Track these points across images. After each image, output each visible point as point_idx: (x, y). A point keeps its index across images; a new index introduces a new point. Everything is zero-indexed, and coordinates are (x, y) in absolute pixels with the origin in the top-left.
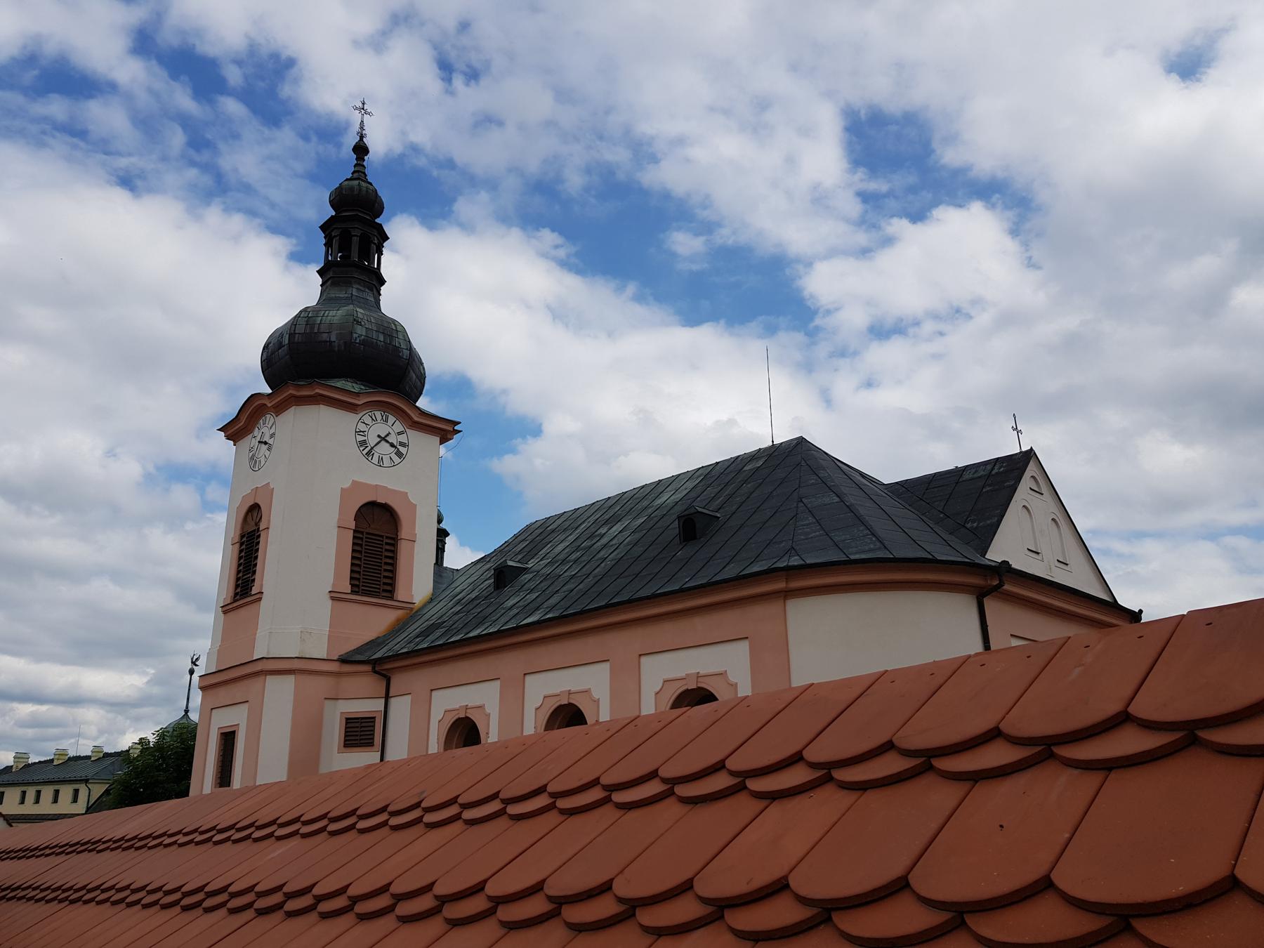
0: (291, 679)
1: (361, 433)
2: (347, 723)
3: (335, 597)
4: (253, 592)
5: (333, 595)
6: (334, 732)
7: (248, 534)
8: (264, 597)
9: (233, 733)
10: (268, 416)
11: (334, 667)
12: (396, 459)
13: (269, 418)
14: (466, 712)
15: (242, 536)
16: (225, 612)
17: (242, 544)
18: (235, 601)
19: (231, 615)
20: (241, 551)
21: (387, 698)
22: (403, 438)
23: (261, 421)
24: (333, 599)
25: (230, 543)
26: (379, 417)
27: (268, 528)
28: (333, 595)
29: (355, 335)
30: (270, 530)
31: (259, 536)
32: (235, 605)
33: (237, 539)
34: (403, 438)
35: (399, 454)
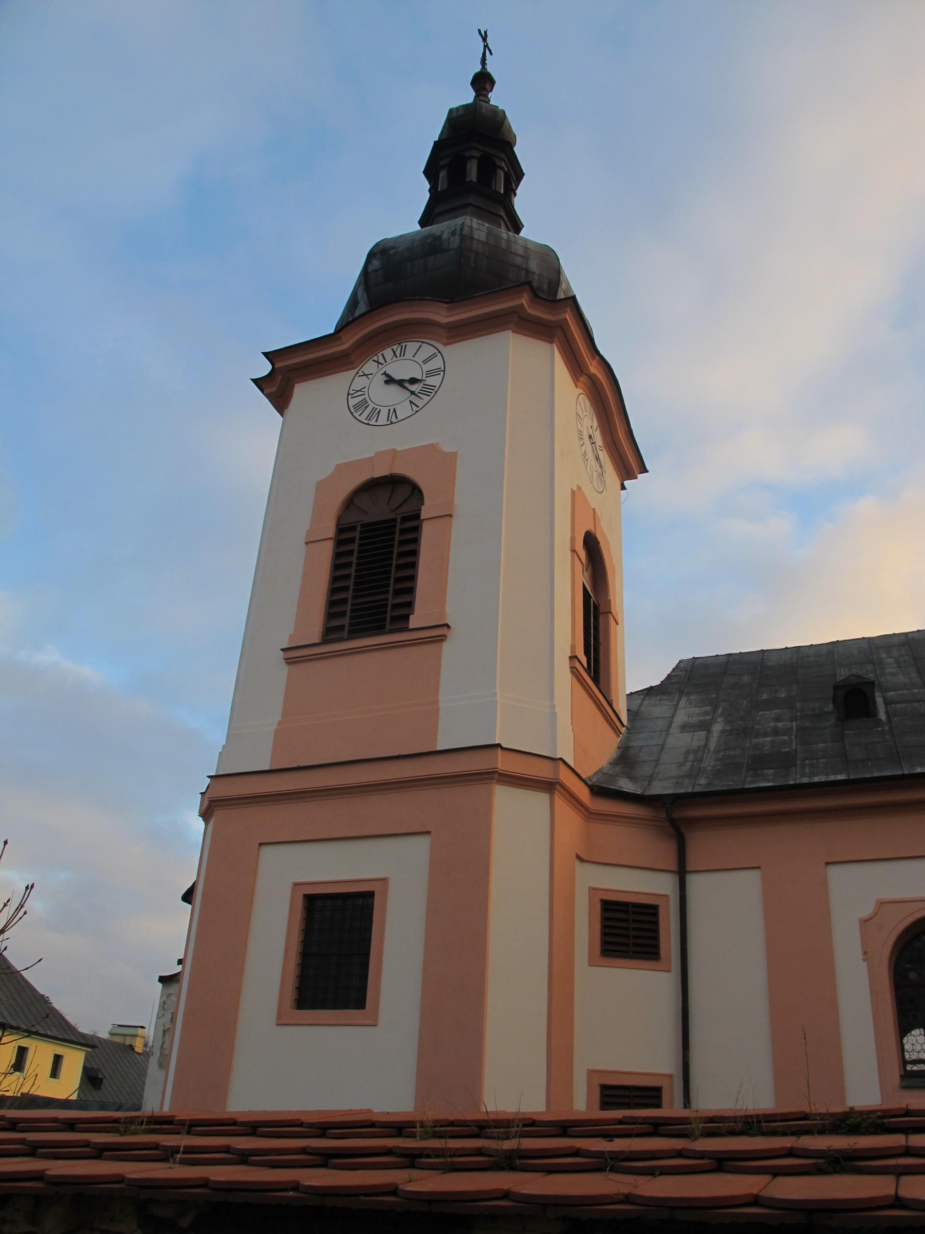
0: (539, 801)
4: (414, 622)
7: (363, 526)
9: (370, 895)
10: (412, 347)
21: (682, 873)
23: (388, 353)
24: (573, 670)
25: (302, 541)
30: (454, 520)
31: (417, 529)
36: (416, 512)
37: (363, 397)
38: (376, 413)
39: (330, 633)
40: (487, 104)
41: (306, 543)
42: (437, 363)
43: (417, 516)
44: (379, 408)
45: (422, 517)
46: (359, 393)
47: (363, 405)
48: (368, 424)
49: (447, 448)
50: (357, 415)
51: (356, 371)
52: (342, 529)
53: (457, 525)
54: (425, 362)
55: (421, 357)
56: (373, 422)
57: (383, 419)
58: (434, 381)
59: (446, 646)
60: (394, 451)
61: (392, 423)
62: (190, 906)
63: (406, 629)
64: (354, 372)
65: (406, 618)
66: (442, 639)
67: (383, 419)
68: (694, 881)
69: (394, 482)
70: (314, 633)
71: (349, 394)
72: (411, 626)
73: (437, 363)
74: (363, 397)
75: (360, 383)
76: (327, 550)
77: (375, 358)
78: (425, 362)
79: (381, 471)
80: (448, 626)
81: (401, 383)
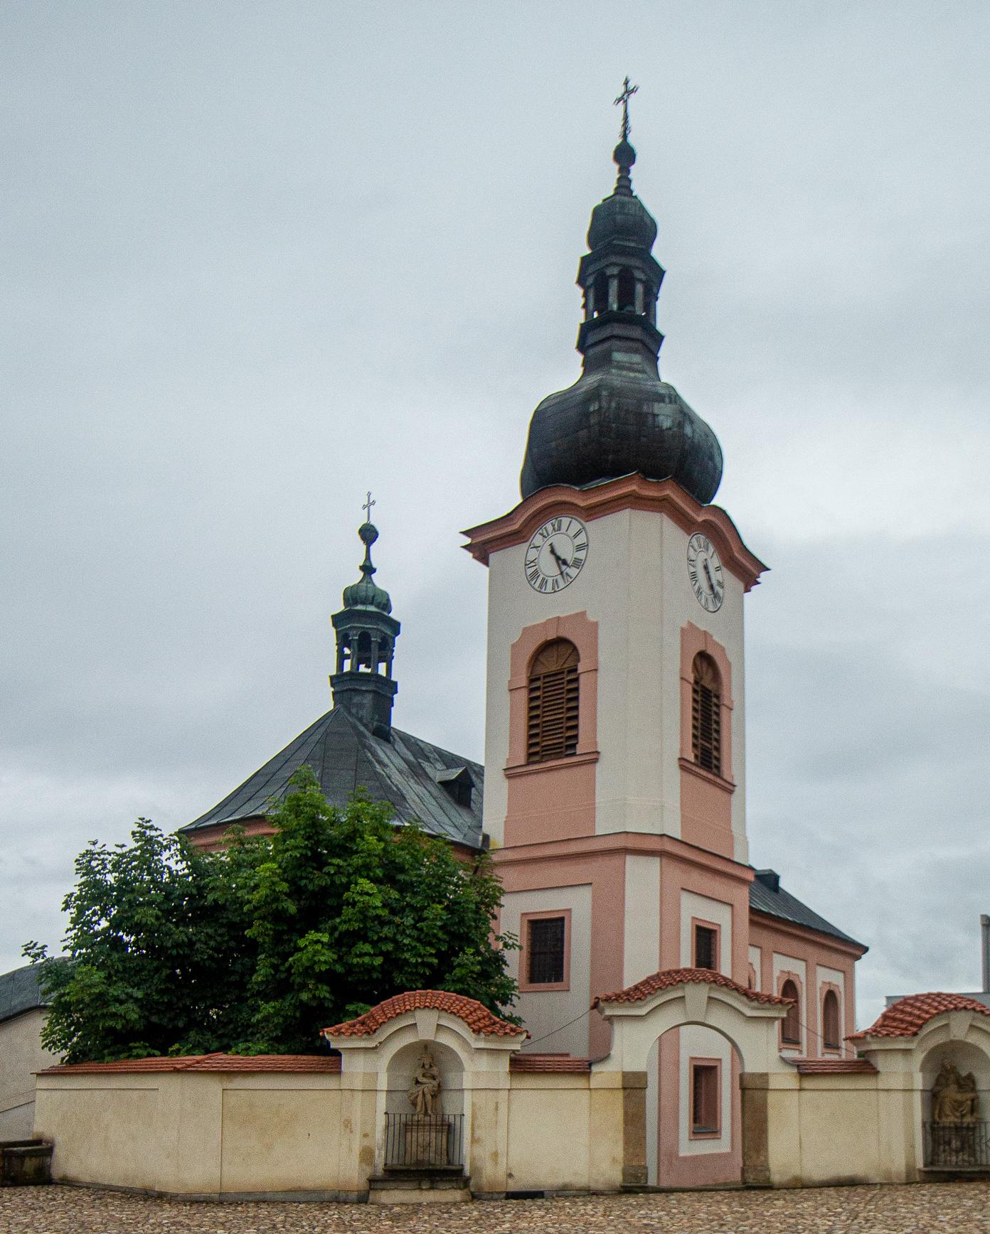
0: (655, 863)
3: (683, 765)
7: (544, 677)
8: (603, 758)
10: (565, 521)
13: (570, 524)
15: (531, 681)
16: (509, 777)
17: (531, 690)
18: (528, 764)
19: (518, 781)
20: (531, 700)
23: (549, 526)
24: (682, 768)
27: (596, 670)
31: (577, 680)
36: (574, 667)
37: (535, 568)
38: (544, 582)
39: (532, 757)
40: (626, 199)
41: (511, 690)
43: (576, 670)
44: (547, 578)
47: (535, 575)
48: (540, 591)
49: (591, 617)
51: (528, 543)
54: (575, 536)
55: (572, 532)
56: (543, 590)
57: (549, 589)
58: (581, 555)
59: (598, 766)
61: (555, 592)
62: (522, 761)
63: (574, 754)
64: (525, 546)
65: (574, 746)
66: (595, 761)
67: (549, 589)
69: (561, 642)
71: (526, 565)
72: (577, 753)
73: (581, 539)
74: (535, 568)
75: (533, 554)
76: (523, 696)
77: (541, 531)
78: (575, 536)
79: (552, 635)
80: (598, 753)
81: (558, 558)
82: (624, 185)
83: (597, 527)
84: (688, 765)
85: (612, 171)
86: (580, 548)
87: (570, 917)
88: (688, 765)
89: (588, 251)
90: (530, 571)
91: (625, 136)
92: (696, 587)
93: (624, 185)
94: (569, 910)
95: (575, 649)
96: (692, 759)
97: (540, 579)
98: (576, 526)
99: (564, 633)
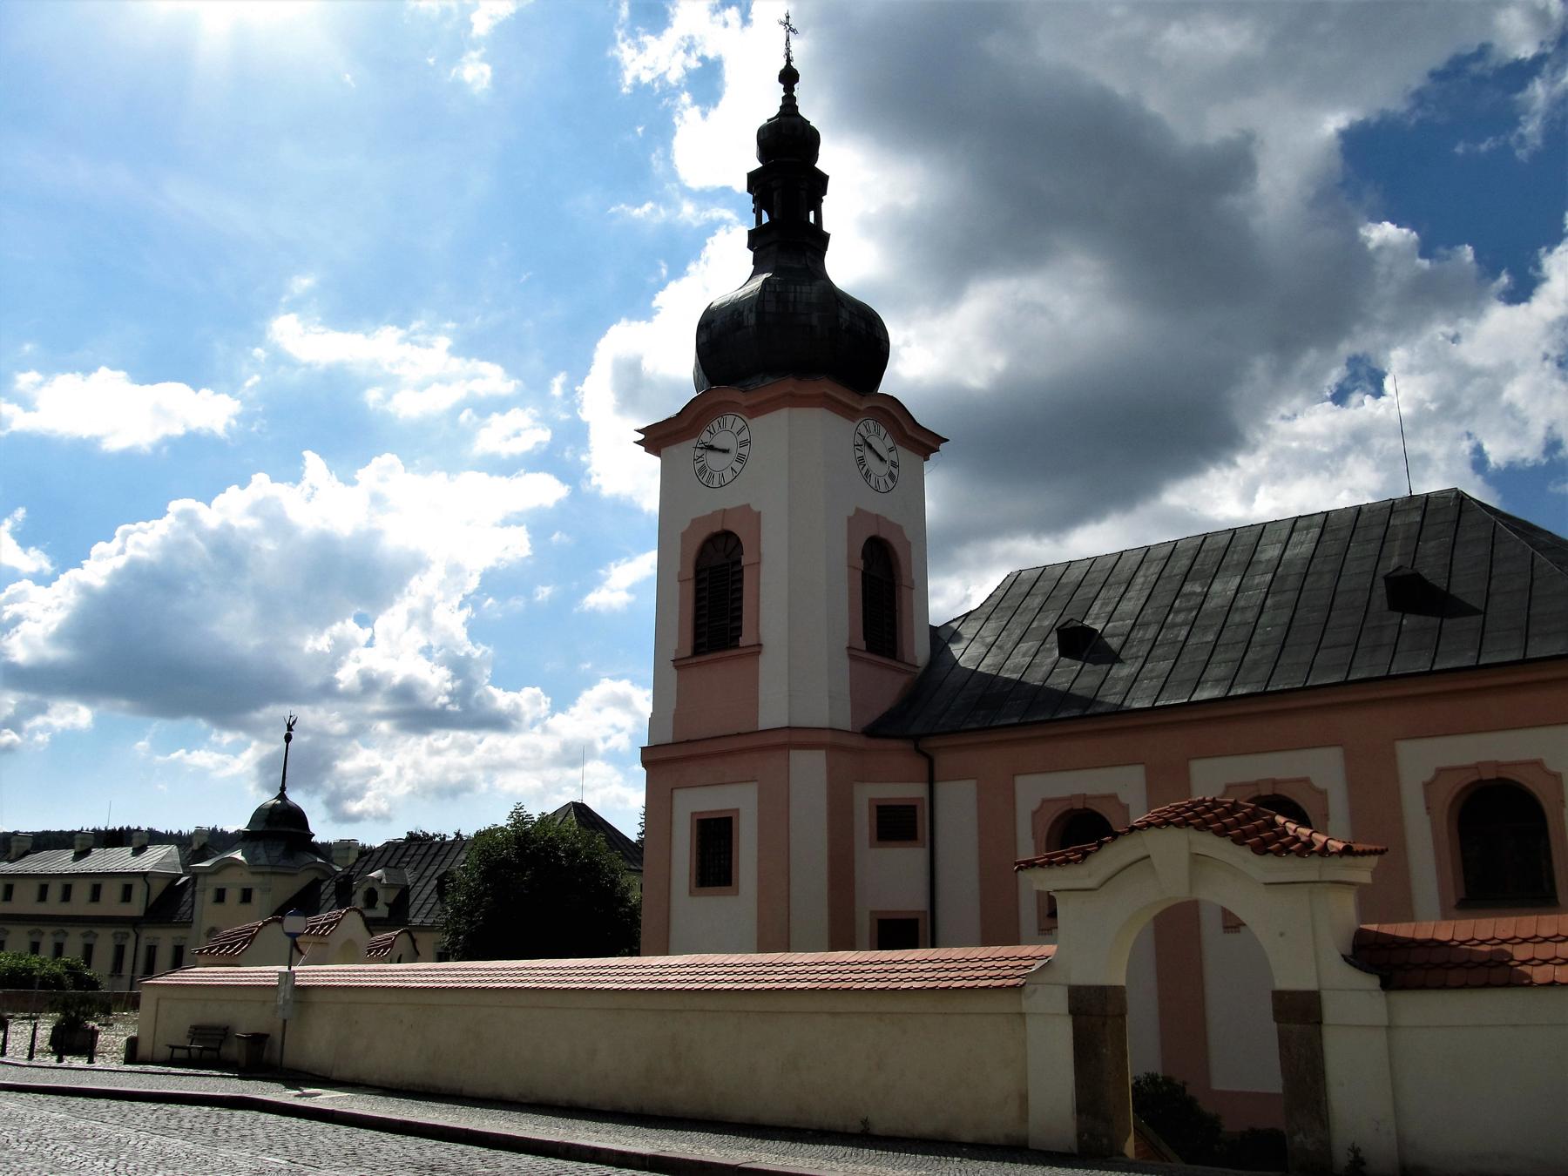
1: (859, 447)
2: (878, 812)
5: (854, 653)
6: (864, 823)
9: (729, 820)
10: (730, 419)
11: (859, 742)
12: (891, 485)
14: (1084, 803)
22: (893, 456)
23: (715, 423)
24: (852, 657)
26: (872, 428)
27: (759, 563)
28: (854, 653)
29: (841, 320)
32: (694, 660)
33: (690, 573)
34: (893, 456)
35: (891, 476)
39: (698, 649)
42: (744, 436)
45: (744, 562)
46: (700, 459)
49: (755, 508)
50: (700, 478)
52: (697, 572)
53: (764, 568)
55: (735, 430)
58: (744, 450)
60: (725, 510)
61: (722, 486)
63: (737, 646)
66: (759, 652)
68: (942, 788)
69: (728, 535)
70: (688, 652)
72: (741, 645)
73: (744, 436)
78: (739, 433)
79: (717, 528)
82: (789, 104)
83: (760, 424)
84: (860, 654)
85: (779, 91)
86: (743, 444)
87: (738, 816)
88: (860, 654)
89: (757, 165)
90: (698, 466)
91: (789, 60)
92: (864, 472)
93: (789, 104)
94: (737, 810)
95: (738, 540)
96: (862, 645)
97: (708, 472)
98: (739, 424)
99: (730, 527)
